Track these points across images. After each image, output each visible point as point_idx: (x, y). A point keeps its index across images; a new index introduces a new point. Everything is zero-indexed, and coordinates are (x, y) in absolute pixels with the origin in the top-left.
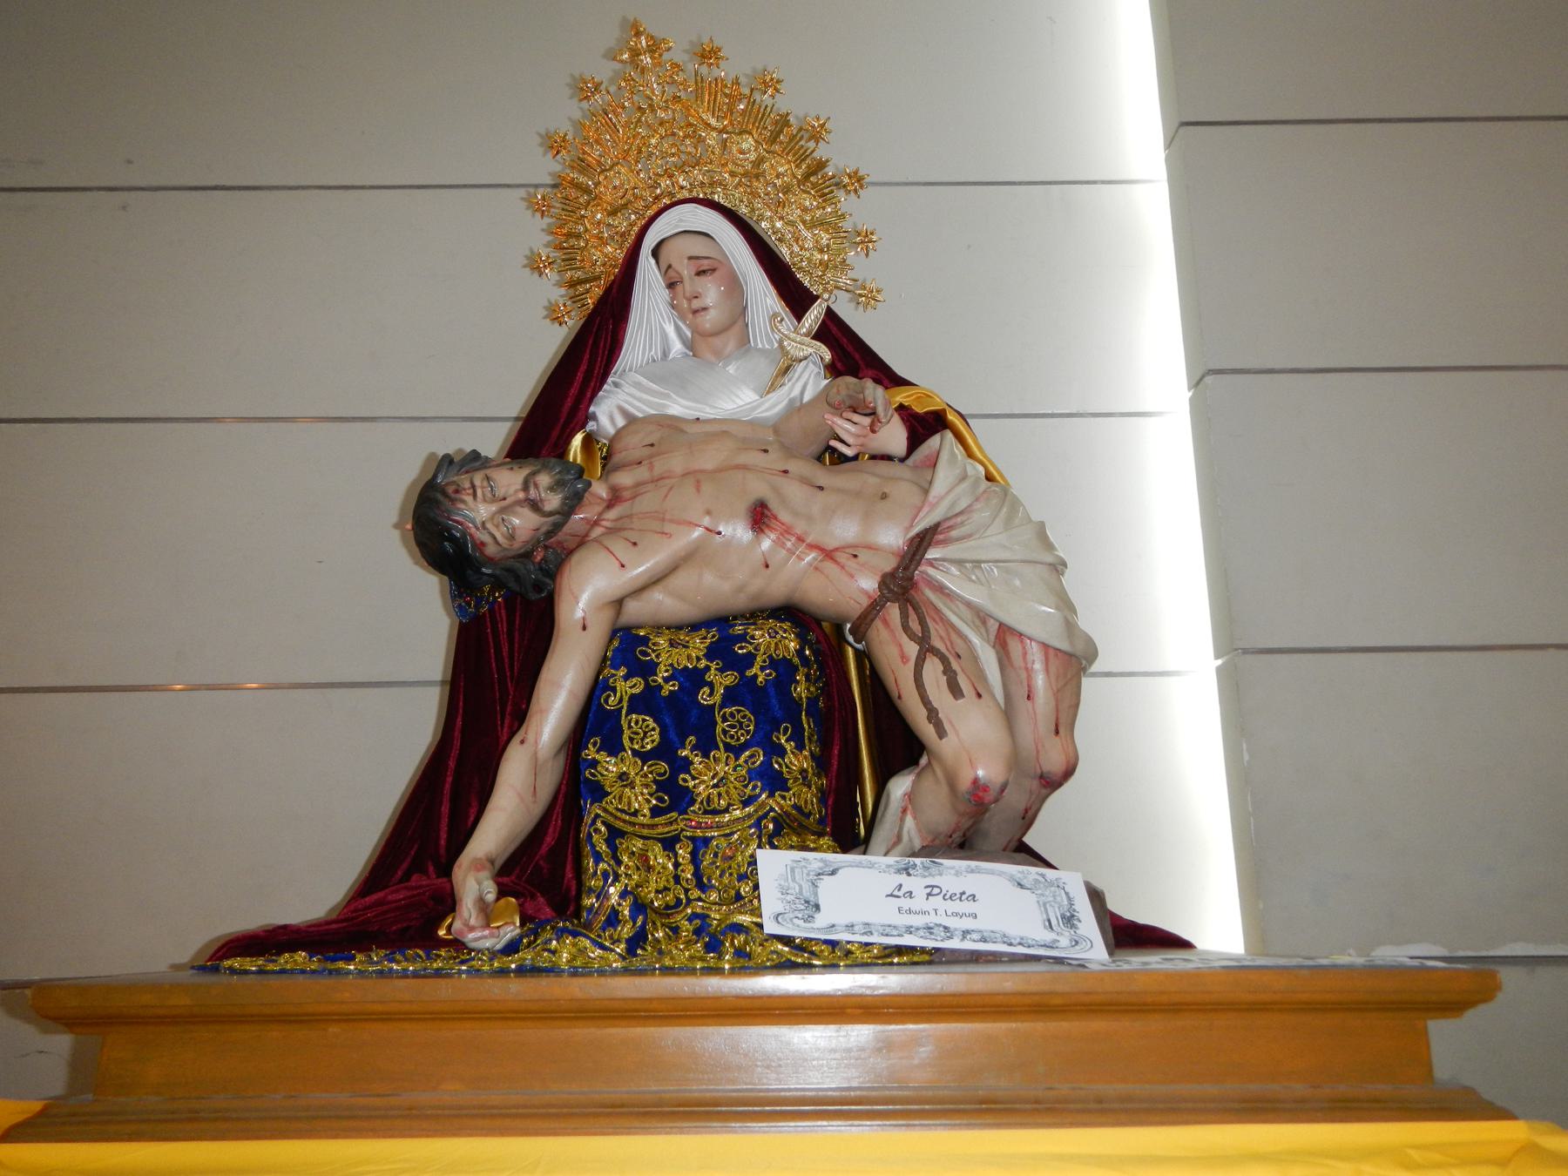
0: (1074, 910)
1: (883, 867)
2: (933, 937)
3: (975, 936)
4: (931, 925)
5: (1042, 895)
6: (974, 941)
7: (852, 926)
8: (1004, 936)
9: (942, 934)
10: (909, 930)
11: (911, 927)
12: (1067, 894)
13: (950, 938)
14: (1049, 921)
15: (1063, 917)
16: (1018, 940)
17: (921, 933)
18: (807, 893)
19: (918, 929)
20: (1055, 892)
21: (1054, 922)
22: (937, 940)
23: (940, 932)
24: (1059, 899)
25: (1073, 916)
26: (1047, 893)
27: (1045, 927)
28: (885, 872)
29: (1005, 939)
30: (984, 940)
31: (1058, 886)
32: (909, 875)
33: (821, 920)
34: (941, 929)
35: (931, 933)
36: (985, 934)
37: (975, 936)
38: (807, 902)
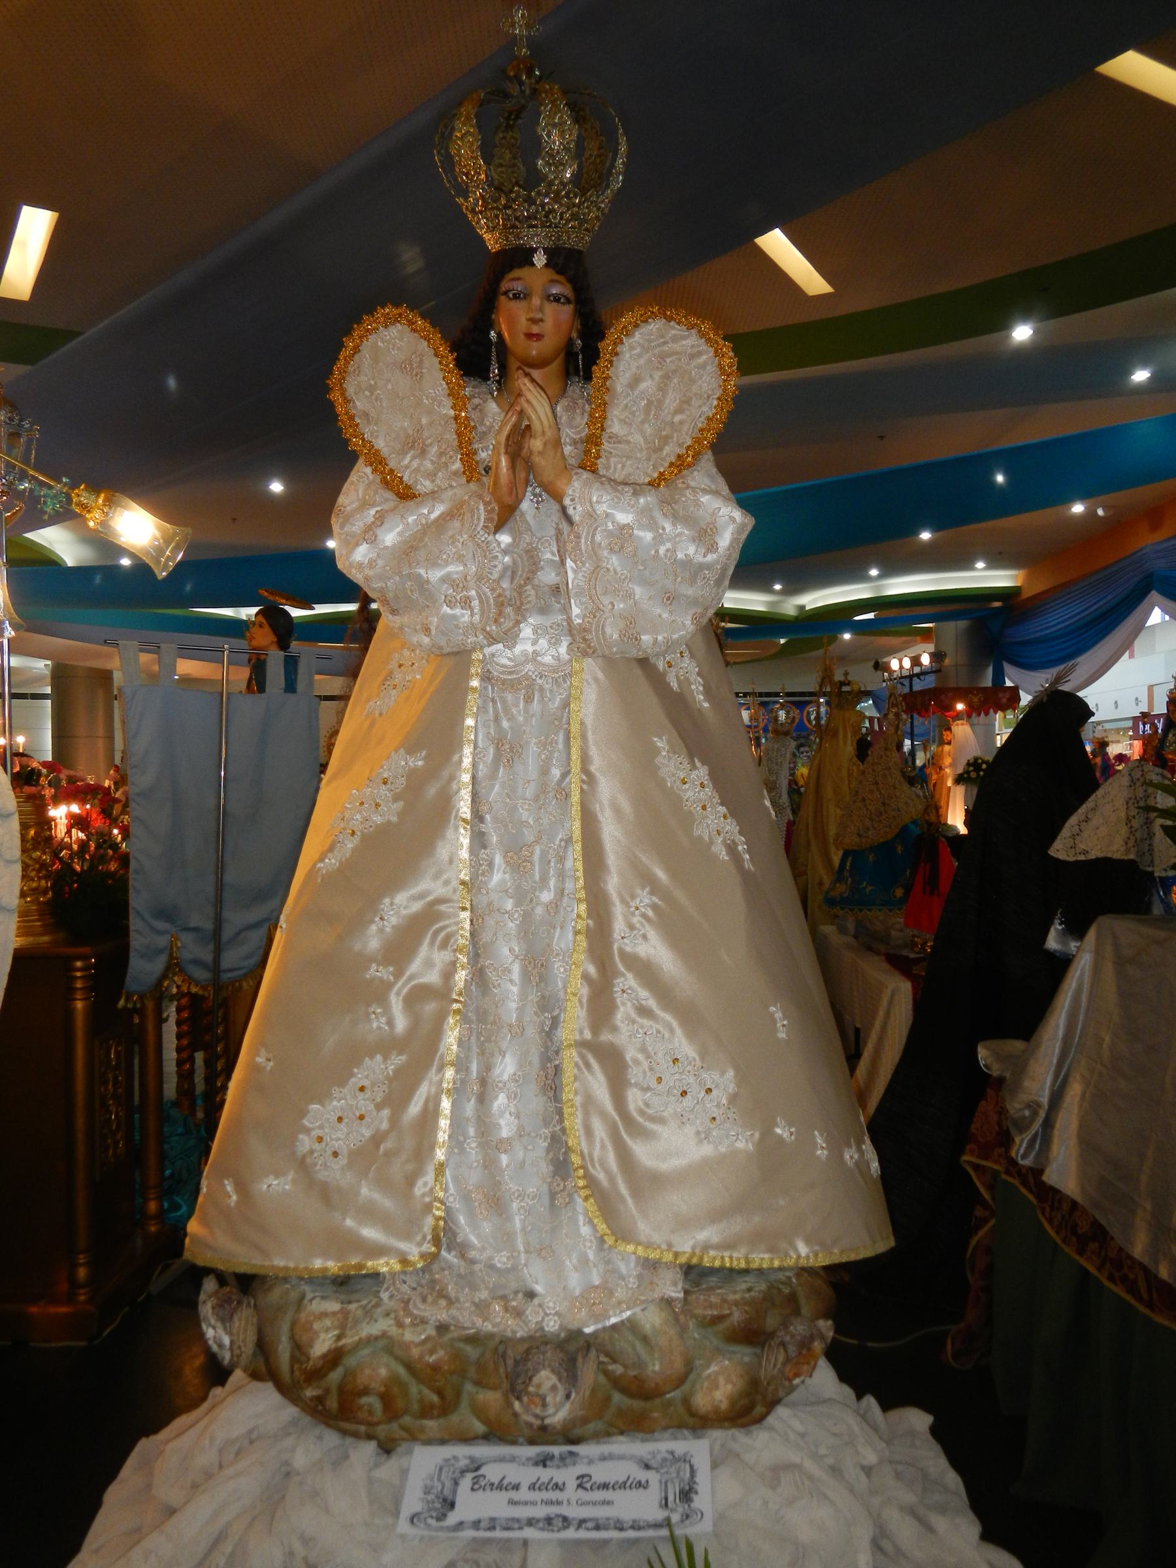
0: (695, 1483)
1: (524, 1460)
2: (551, 1528)
3: (590, 1525)
4: (553, 1516)
5: (667, 1473)
6: (588, 1529)
7: (479, 1521)
8: (618, 1521)
9: (560, 1524)
10: (531, 1522)
11: (533, 1519)
12: (691, 1467)
13: (565, 1528)
14: (666, 1499)
15: (681, 1492)
16: (631, 1523)
17: (541, 1525)
18: (447, 1492)
19: (538, 1521)
20: (680, 1467)
21: (671, 1498)
22: (553, 1531)
23: (558, 1523)
24: (681, 1473)
25: (691, 1489)
26: (673, 1470)
27: (661, 1506)
28: (524, 1464)
29: (618, 1525)
30: (597, 1528)
31: (685, 1461)
32: (545, 1466)
33: (453, 1518)
34: (560, 1519)
35: (550, 1524)
36: (600, 1522)
37: (590, 1525)
38: (445, 1500)
